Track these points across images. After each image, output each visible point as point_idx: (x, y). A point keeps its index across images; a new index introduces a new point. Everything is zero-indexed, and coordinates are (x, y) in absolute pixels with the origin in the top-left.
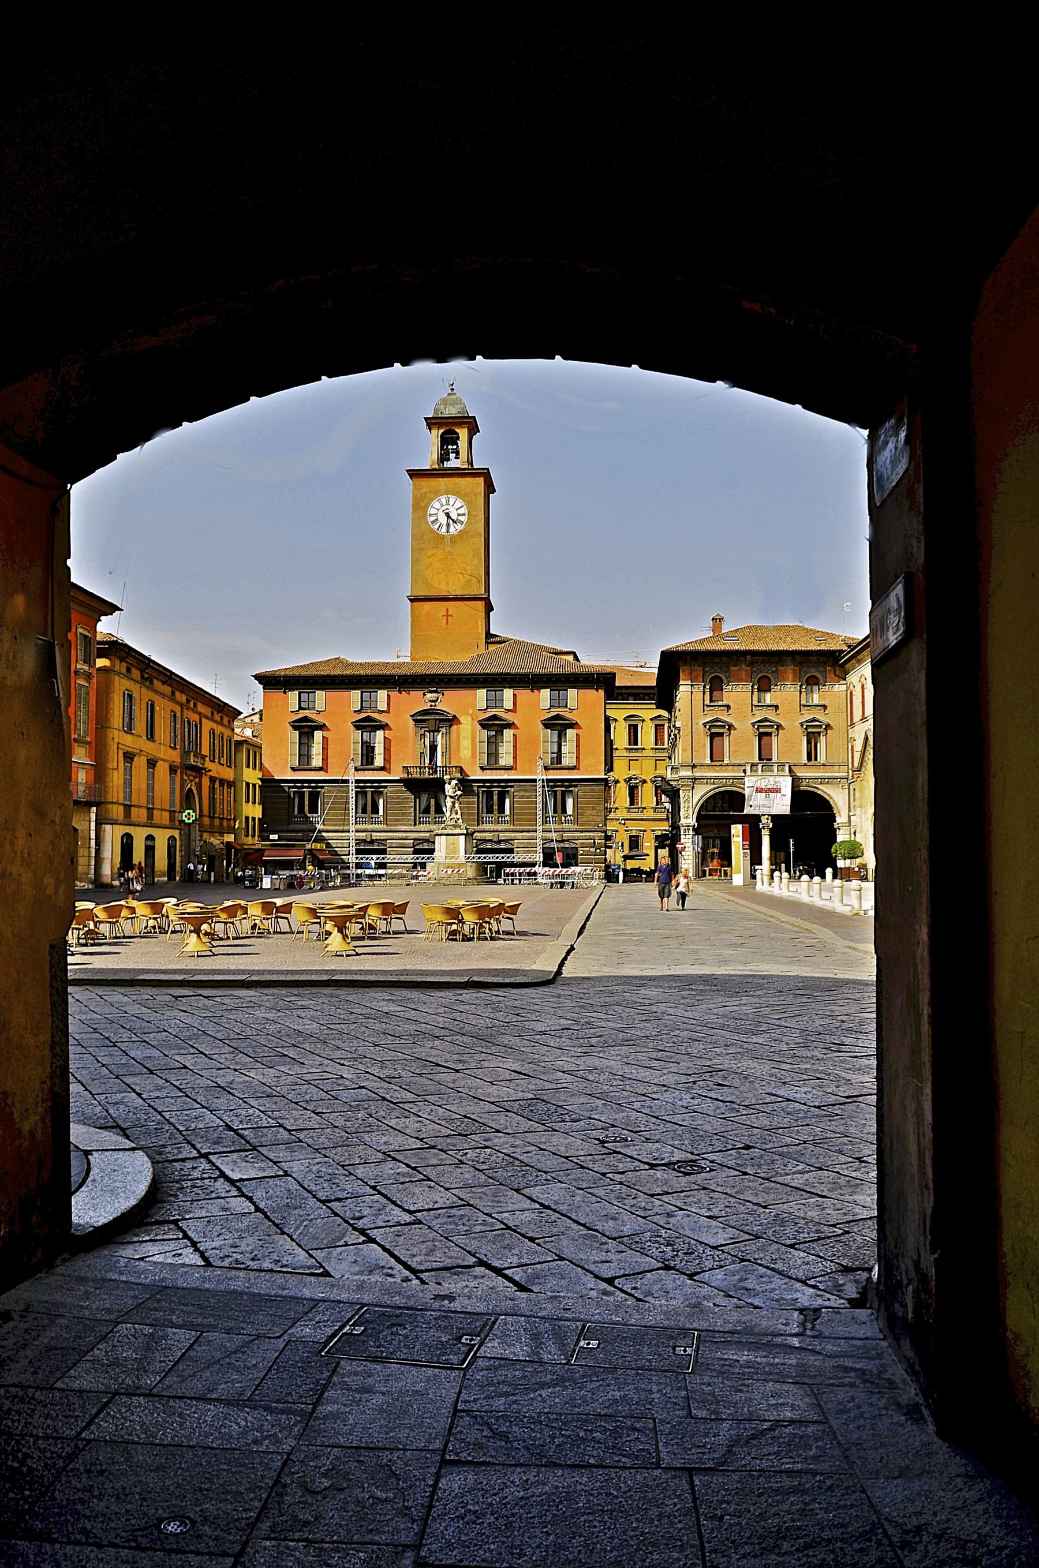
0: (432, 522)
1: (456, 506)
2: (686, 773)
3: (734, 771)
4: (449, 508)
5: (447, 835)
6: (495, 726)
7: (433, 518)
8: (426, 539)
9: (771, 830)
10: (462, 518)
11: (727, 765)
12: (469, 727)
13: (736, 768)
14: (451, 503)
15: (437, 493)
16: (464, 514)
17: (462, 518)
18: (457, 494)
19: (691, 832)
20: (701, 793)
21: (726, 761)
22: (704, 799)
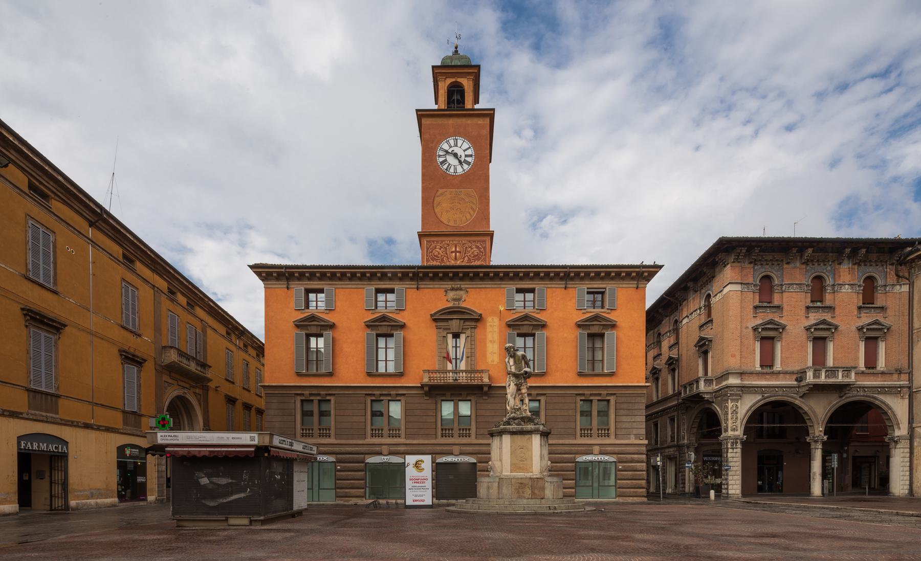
0: (442, 163)
1: (463, 147)
2: (733, 381)
3: (785, 379)
4: (457, 151)
5: (513, 433)
6: (525, 326)
7: (441, 159)
8: (434, 179)
9: (824, 443)
10: (469, 159)
11: (779, 373)
12: (496, 329)
13: (788, 376)
14: (459, 145)
15: (445, 136)
16: (471, 156)
17: (469, 159)
18: (467, 137)
19: (739, 446)
20: (744, 406)
21: (778, 367)
22: (753, 409)
